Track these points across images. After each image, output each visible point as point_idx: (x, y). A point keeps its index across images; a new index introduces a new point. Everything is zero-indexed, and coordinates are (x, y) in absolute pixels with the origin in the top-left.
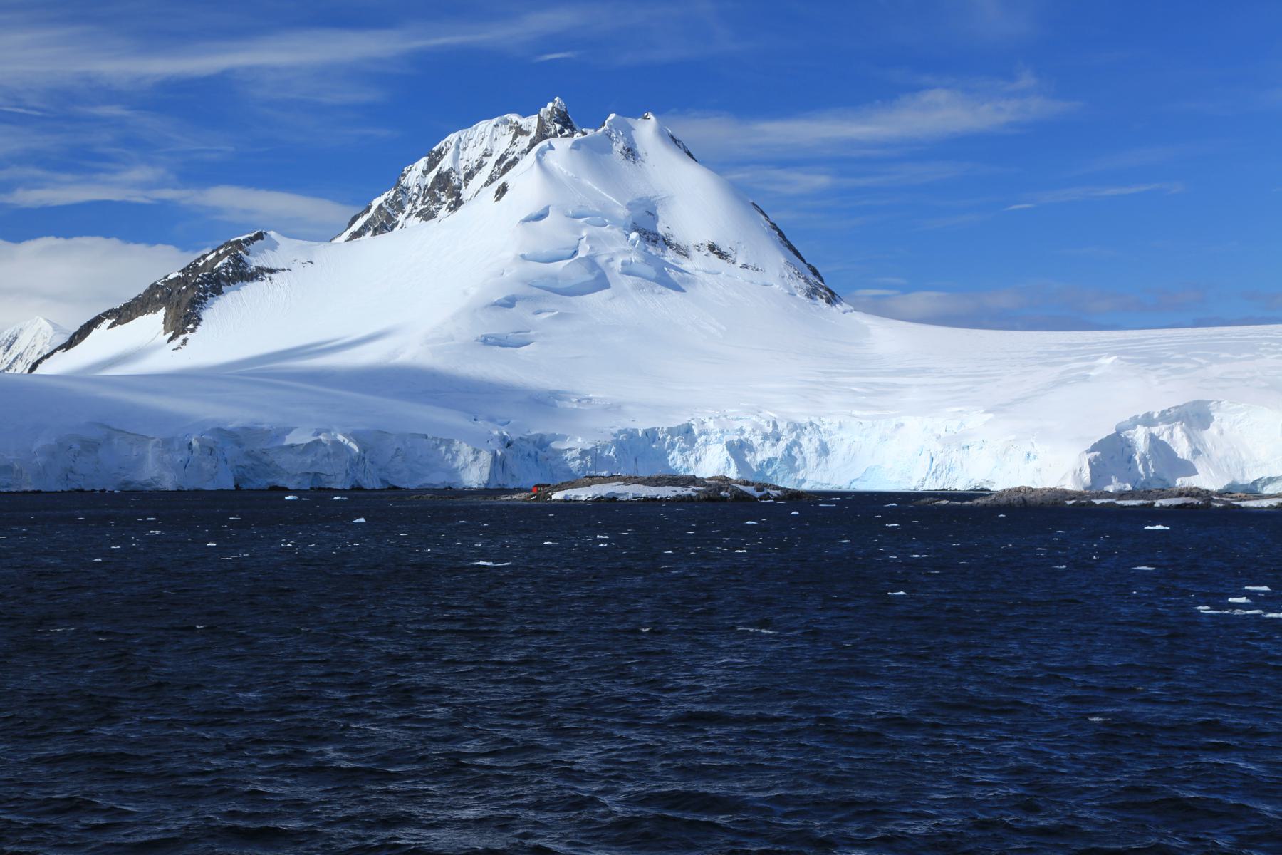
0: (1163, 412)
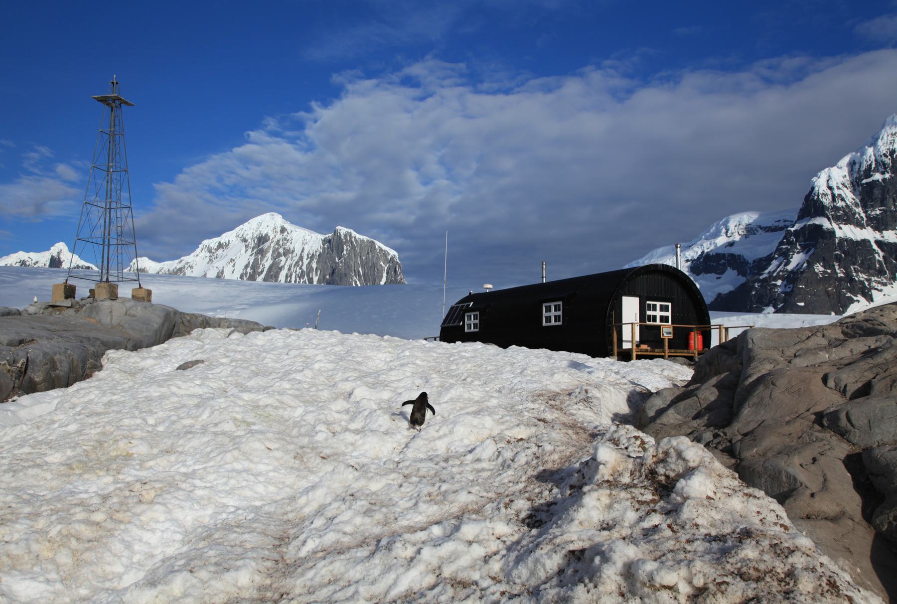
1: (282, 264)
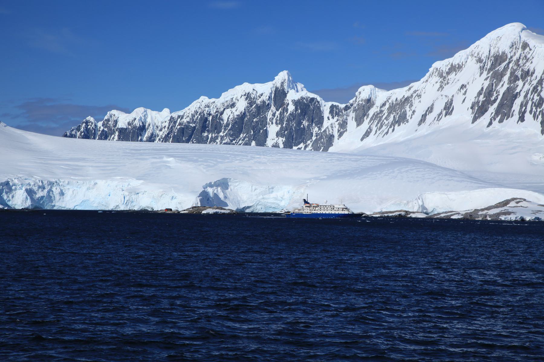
0: (215, 182)
1: (518, 90)
